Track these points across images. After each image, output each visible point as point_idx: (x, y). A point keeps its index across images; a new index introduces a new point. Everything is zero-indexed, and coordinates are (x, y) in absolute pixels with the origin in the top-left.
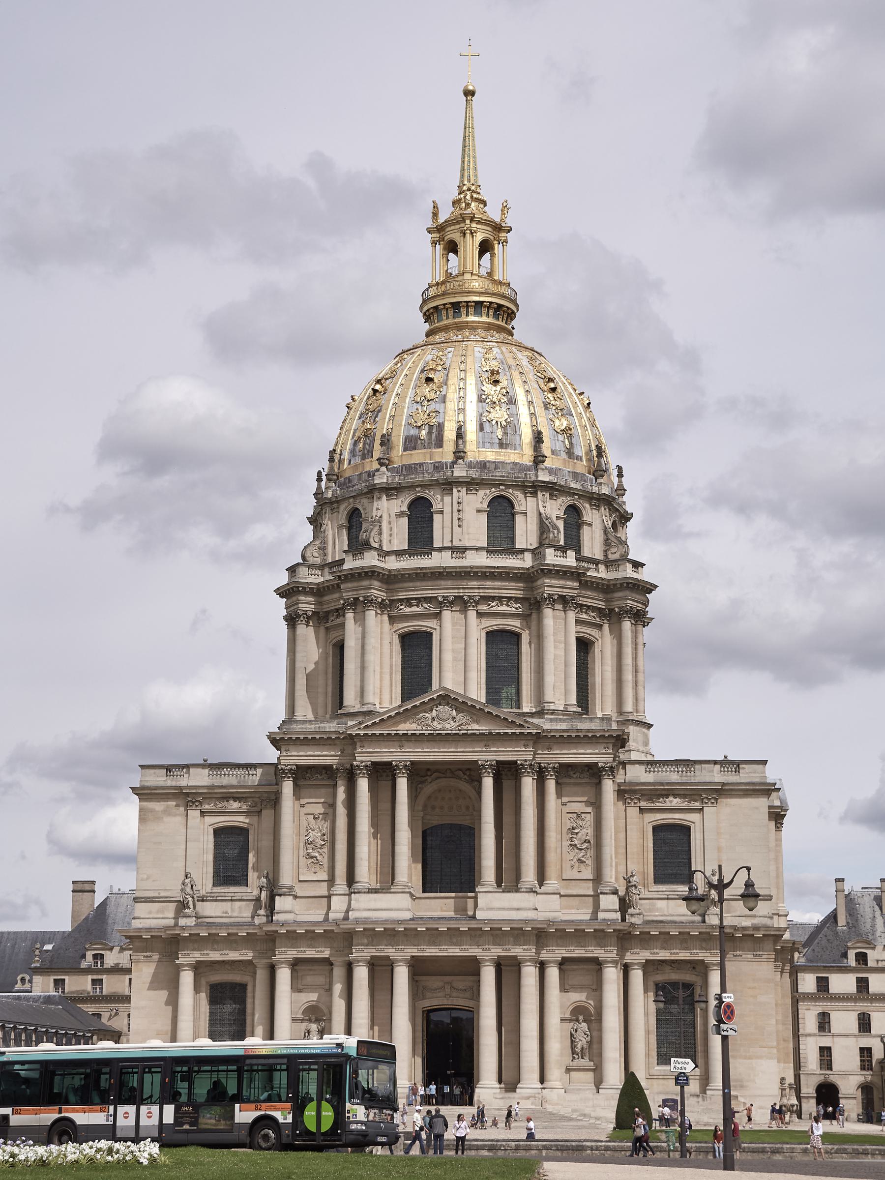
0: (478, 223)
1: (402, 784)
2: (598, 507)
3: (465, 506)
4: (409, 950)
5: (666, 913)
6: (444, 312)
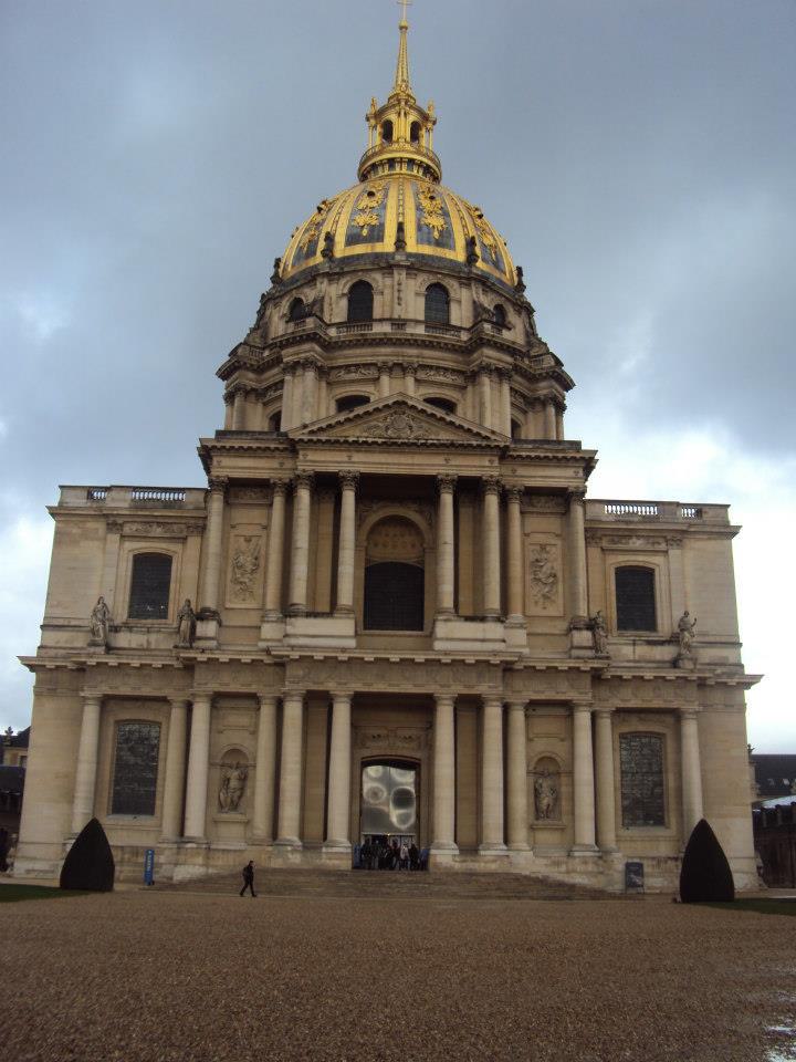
0: (411, 107)
1: (349, 497)
2: (520, 313)
3: (403, 287)
4: (353, 685)
5: (632, 658)
6: (380, 169)
